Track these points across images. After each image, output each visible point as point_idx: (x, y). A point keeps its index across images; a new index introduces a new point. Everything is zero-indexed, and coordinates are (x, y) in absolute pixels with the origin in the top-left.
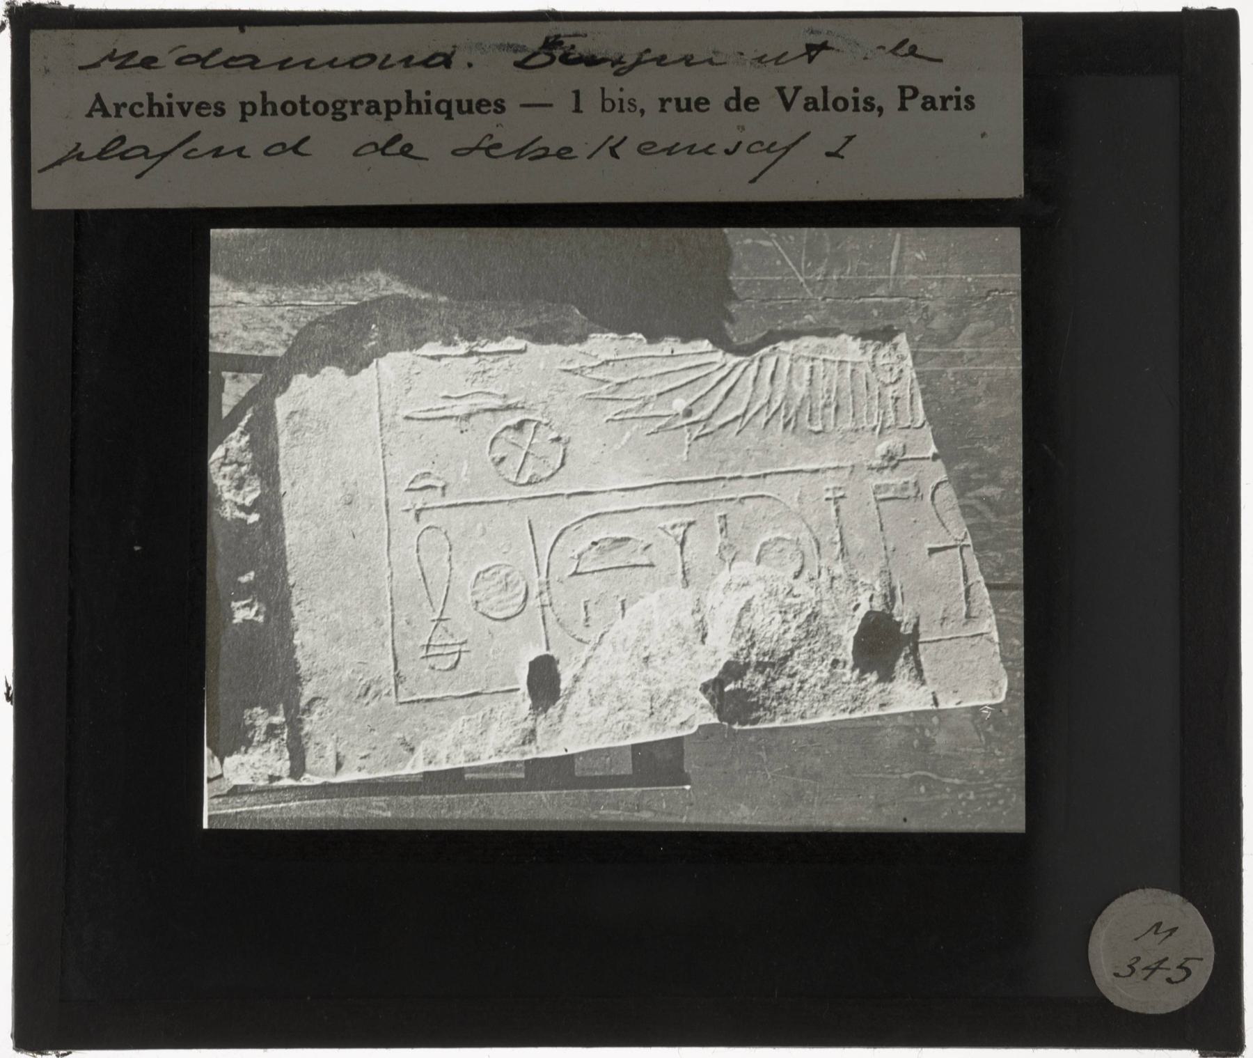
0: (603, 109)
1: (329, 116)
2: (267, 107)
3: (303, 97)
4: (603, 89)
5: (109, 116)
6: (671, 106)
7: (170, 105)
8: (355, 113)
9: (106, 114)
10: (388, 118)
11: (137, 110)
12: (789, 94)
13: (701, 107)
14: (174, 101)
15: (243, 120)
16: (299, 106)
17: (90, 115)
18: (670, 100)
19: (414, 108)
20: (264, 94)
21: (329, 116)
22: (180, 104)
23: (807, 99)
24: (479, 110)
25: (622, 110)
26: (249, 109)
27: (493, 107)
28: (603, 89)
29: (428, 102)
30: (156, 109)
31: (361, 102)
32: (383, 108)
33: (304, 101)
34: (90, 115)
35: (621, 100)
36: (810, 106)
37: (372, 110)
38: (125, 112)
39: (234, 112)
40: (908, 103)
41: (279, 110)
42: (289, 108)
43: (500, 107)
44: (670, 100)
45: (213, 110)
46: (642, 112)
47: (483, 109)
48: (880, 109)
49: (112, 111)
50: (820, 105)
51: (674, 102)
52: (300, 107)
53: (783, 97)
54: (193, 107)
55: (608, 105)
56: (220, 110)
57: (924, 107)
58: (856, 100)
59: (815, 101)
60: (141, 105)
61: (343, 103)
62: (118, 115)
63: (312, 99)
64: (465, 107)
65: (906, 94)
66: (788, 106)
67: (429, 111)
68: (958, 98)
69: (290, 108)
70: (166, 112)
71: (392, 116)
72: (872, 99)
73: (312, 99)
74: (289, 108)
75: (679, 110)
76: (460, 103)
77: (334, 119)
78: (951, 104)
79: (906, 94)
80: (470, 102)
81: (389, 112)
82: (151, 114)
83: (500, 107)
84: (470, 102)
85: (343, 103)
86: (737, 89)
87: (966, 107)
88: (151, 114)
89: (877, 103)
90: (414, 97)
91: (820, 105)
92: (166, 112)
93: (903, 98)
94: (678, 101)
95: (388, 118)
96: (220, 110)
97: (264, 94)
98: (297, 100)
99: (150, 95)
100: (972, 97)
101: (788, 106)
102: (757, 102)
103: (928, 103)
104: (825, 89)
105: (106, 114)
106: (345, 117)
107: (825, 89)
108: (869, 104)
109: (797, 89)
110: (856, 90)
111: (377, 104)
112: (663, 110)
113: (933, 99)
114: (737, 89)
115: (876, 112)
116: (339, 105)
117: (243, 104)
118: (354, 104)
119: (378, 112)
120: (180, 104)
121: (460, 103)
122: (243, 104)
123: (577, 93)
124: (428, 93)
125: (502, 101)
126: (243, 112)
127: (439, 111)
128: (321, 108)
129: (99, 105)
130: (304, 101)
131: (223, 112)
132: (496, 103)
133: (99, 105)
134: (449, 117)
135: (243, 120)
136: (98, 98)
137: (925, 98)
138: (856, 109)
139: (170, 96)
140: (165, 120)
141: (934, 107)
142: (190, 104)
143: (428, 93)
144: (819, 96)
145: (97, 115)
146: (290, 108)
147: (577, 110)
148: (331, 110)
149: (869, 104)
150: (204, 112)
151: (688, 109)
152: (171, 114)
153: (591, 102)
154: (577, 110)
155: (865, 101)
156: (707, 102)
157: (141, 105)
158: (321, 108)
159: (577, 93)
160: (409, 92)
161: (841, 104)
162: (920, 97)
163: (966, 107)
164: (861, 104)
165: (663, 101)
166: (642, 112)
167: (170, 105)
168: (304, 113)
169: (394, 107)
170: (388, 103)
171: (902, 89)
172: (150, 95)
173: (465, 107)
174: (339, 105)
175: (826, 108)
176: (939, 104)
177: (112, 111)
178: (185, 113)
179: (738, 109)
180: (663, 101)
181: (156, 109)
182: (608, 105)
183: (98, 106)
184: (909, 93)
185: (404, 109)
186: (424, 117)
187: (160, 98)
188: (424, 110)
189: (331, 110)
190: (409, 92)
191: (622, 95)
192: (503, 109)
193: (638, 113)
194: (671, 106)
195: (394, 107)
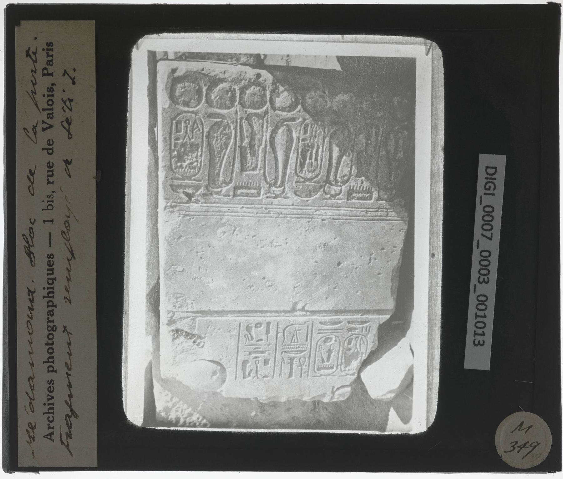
0: (52, 210)
1: (54, 333)
2: (50, 360)
3: (46, 344)
4: (43, 210)
6: (51, 179)
7: (49, 404)
8: (53, 321)
10: (55, 306)
11: (51, 419)
12: (45, 126)
13: (51, 165)
14: (47, 403)
15: (56, 372)
16: (49, 346)
17: (53, 441)
18: (48, 180)
19: (50, 295)
20: (44, 362)
21: (54, 333)
22: (49, 400)
23: (48, 118)
25: (52, 201)
26: (51, 369)
27: (51, 259)
28: (43, 210)
29: (48, 288)
30: (51, 411)
31: (48, 318)
32: (51, 309)
33: (47, 344)
35: (48, 201)
36: (51, 116)
38: (52, 425)
39: (52, 376)
40: (49, 72)
42: (50, 351)
43: (51, 256)
44: (48, 180)
45: (51, 385)
46: (53, 192)
47: (51, 264)
48: (53, 85)
49: (51, 431)
50: (51, 112)
51: (49, 178)
52: (50, 346)
53: (47, 128)
55: (50, 207)
56: (51, 382)
57: (52, 65)
58: (48, 96)
59: (49, 114)
60: (49, 417)
61: (48, 326)
62: (53, 428)
63: (46, 341)
64: (51, 272)
66: (51, 126)
67: (53, 288)
69: (51, 351)
70: (52, 406)
71: (54, 304)
72: (48, 88)
73: (46, 341)
74: (50, 351)
75: (52, 176)
76: (48, 274)
77: (55, 331)
78: (51, 53)
80: (48, 270)
81: (53, 306)
82: (53, 413)
83: (51, 256)
84: (48, 270)
86: (43, 149)
87: (52, 46)
88: (53, 413)
89: (50, 86)
90: (46, 295)
91: (51, 112)
92: (52, 406)
93: (48, 74)
94: (48, 176)
95: (55, 306)
96: (51, 382)
97: (44, 362)
98: (47, 347)
99: (44, 413)
100: (47, 43)
101: (51, 126)
102: (49, 140)
103: (50, 63)
104: (44, 110)
106: (55, 326)
107: (44, 110)
108: (50, 89)
109: (43, 122)
112: (53, 183)
113: (48, 61)
114: (43, 149)
115: (54, 87)
116: (49, 329)
117: (49, 371)
118: (49, 321)
119: (52, 311)
120: (49, 400)
121: (48, 274)
122: (49, 371)
123: (45, 221)
124: (44, 288)
125: (48, 255)
126: (53, 371)
127: (53, 283)
128: (51, 337)
129: (49, 436)
130: (47, 344)
131: (52, 380)
132: (49, 258)
133: (49, 436)
137: (48, 65)
138: (53, 96)
139: (45, 404)
141: (52, 60)
142: (48, 395)
143: (44, 288)
146: (51, 351)
147: (52, 221)
148: (51, 332)
149: (50, 89)
150: (52, 390)
151: (52, 171)
152: (53, 404)
153: (48, 215)
154: (52, 221)
155: (49, 91)
156: (49, 163)
157: (49, 417)
158: (51, 336)
159: (45, 221)
160: (44, 297)
161: (50, 103)
162: (46, 66)
163: (52, 46)
164: (51, 93)
165: (49, 183)
166: (53, 192)
167: (49, 404)
168: (53, 344)
169: (50, 304)
170: (48, 306)
171: (43, 75)
172: (44, 413)
173: (51, 272)
174: (49, 329)
175: (52, 109)
176: (50, 58)
177: (51, 431)
178: (52, 398)
179: (52, 149)
180: (49, 183)
181: (50, 411)
182: (50, 207)
183: (49, 437)
184: (45, 72)
185: (51, 299)
187: (46, 409)
188: (51, 290)
189: (51, 332)
190: (44, 297)
191: (46, 201)
192: (52, 254)
193: (54, 194)
194: (51, 179)
195: (50, 304)
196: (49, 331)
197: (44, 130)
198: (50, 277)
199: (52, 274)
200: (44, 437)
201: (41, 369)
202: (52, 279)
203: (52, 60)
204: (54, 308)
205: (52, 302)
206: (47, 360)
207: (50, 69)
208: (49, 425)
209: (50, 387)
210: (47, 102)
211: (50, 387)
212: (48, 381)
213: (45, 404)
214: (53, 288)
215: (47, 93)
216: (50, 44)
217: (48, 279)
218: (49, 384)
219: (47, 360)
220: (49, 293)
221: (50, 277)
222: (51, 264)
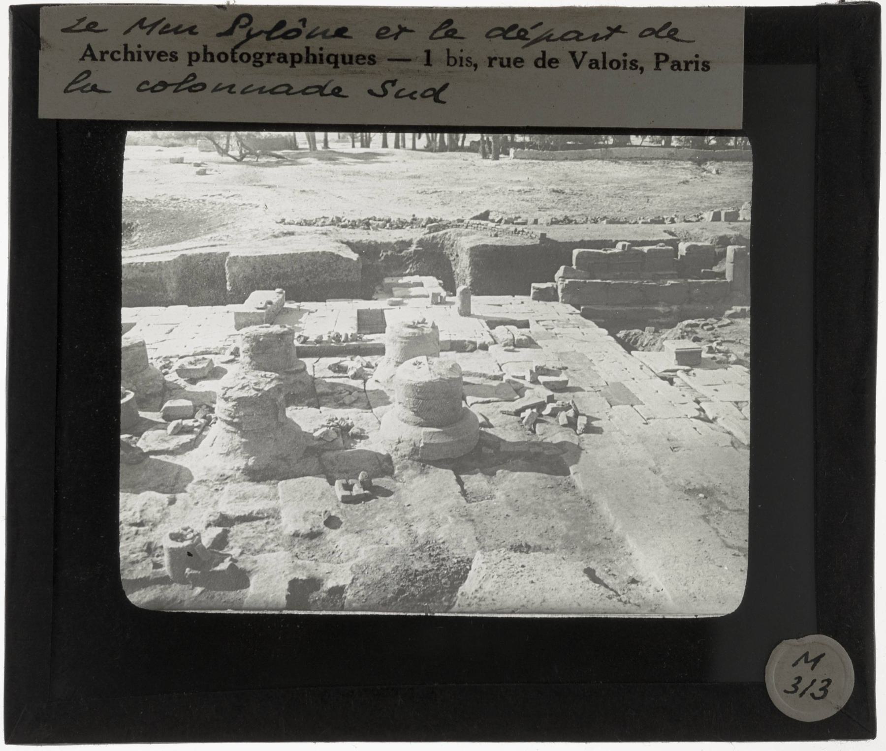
1: (251, 63)
5: (97, 60)
7: (139, 53)
9: (94, 58)
10: (293, 66)
11: (116, 56)
12: (579, 57)
13: (518, 64)
14: (142, 49)
15: (190, 64)
16: (230, 57)
17: (82, 59)
20: (205, 47)
21: (251, 63)
22: (147, 53)
23: (591, 60)
24: (357, 62)
26: (194, 57)
29: (321, 55)
30: (129, 56)
31: (274, 54)
32: (289, 59)
34: (82, 59)
37: (282, 60)
38: (107, 57)
39: (183, 58)
41: (216, 59)
42: (223, 58)
45: (169, 57)
47: (360, 61)
48: (642, 69)
49: (98, 55)
50: (601, 65)
53: (575, 60)
54: (155, 55)
56: (174, 57)
57: (672, 68)
58: (625, 61)
59: (597, 62)
60: (119, 52)
61: (261, 55)
62: (102, 59)
64: (347, 60)
65: (660, 59)
66: (577, 66)
68: (697, 63)
71: (296, 65)
72: (636, 61)
74: (223, 58)
76: (343, 56)
77: (254, 65)
78: (692, 67)
79: (660, 59)
80: (351, 57)
81: (293, 62)
82: (126, 59)
83: (372, 60)
85: (261, 55)
88: (126, 59)
91: (601, 65)
95: (293, 66)
96: (174, 57)
97: (205, 47)
99: (126, 46)
101: (577, 66)
103: (676, 66)
104: (604, 54)
105: (94, 58)
106: (262, 64)
107: (604, 54)
108: (634, 64)
109: (584, 53)
110: (625, 55)
111: (285, 56)
115: (638, 71)
116: (258, 56)
118: (269, 55)
119: (286, 62)
120: (147, 53)
121: (343, 56)
122: (190, 54)
128: (245, 58)
131: (176, 59)
134: (336, 67)
135: (190, 64)
136: (89, 47)
137: (673, 62)
138: (625, 68)
139: (139, 46)
140: (136, 63)
142: (154, 52)
143: (321, 49)
144: (600, 59)
145: (88, 59)
148: (252, 59)
149: (634, 64)
150: (163, 58)
152: (140, 60)
155: (631, 63)
157: (119, 52)
160: (308, 48)
161: (615, 65)
162: (670, 60)
163: (703, 69)
164: (628, 65)
167: (139, 53)
168: (234, 61)
169: (297, 58)
170: (293, 55)
171: (658, 55)
172: (126, 46)
173: (347, 60)
174: (258, 56)
175: (604, 68)
176: (683, 66)
178: (150, 59)
183: (88, 53)
184: (662, 58)
185: (304, 60)
186: (318, 66)
187: (132, 48)
189: (252, 59)
195: (297, 58)
196: (254, 55)
197: (573, 54)
198: (340, 59)
199: (344, 62)
200: (89, 47)
201: (195, 44)
202: (336, 62)
203: (680, 70)
204: (290, 64)
205: (300, 61)
206: (208, 51)
207: (666, 67)
208: (107, 52)
209: (166, 55)
210: (614, 60)
211: (166, 55)
212: (176, 53)
213: (139, 46)
214: (321, 62)
215: (628, 59)
216: (706, 66)
217: (336, 56)
218: (171, 54)
219: (208, 51)
220: (314, 56)
221: (340, 59)
222: (360, 61)
